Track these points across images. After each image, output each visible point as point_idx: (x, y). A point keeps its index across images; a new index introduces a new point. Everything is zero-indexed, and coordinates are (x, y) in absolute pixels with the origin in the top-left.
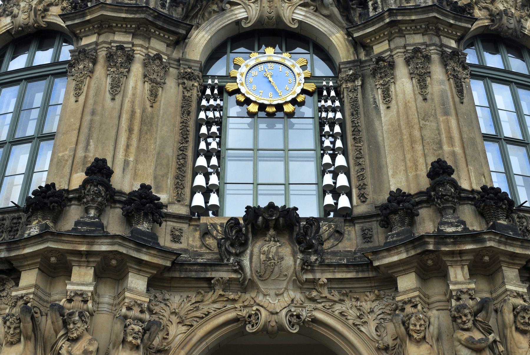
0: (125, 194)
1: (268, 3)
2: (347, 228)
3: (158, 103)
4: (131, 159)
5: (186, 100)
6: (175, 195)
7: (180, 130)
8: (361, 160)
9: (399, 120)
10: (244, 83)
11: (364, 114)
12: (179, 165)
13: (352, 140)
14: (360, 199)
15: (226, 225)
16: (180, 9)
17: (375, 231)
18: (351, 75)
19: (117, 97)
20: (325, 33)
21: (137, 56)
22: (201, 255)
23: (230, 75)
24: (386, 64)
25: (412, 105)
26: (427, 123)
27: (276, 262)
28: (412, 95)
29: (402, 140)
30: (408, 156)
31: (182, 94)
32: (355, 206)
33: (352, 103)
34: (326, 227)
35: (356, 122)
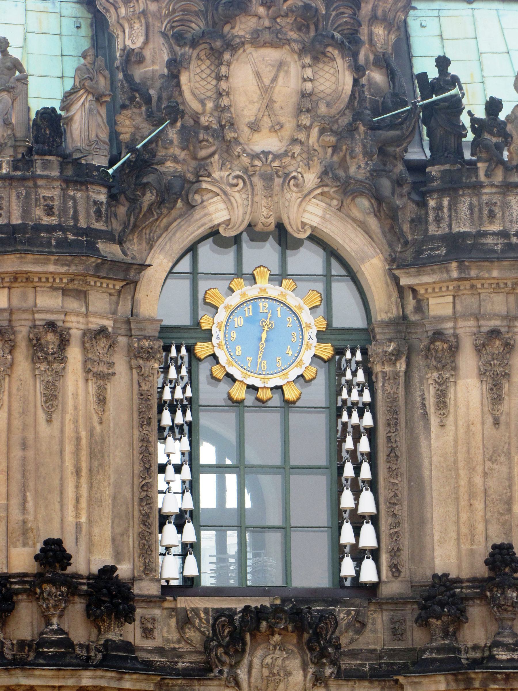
0: (80, 577)
1: (265, 200)
2: (372, 614)
3: (107, 413)
4: (83, 519)
5: (143, 397)
6: (142, 565)
7: (141, 454)
8: (397, 507)
9: (456, 453)
10: (223, 343)
11: (406, 423)
12: (144, 516)
13: (386, 471)
14: (391, 570)
15: (216, 619)
16: (122, 210)
17: (408, 624)
18: (392, 354)
19: (54, 416)
20: (353, 254)
21: (73, 332)
22: (180, 656)
23: (201, 327)
24: (445, 346)
25: (477, 428)
26: (494, 466)
27: (282, 679)
28: (480, 413)
29: (457, 488)
30: (464, 516)
31: (137, 387)
32: (385, 582)
33: (389, 405)
34: (344, 614)
35: (393, 440)
